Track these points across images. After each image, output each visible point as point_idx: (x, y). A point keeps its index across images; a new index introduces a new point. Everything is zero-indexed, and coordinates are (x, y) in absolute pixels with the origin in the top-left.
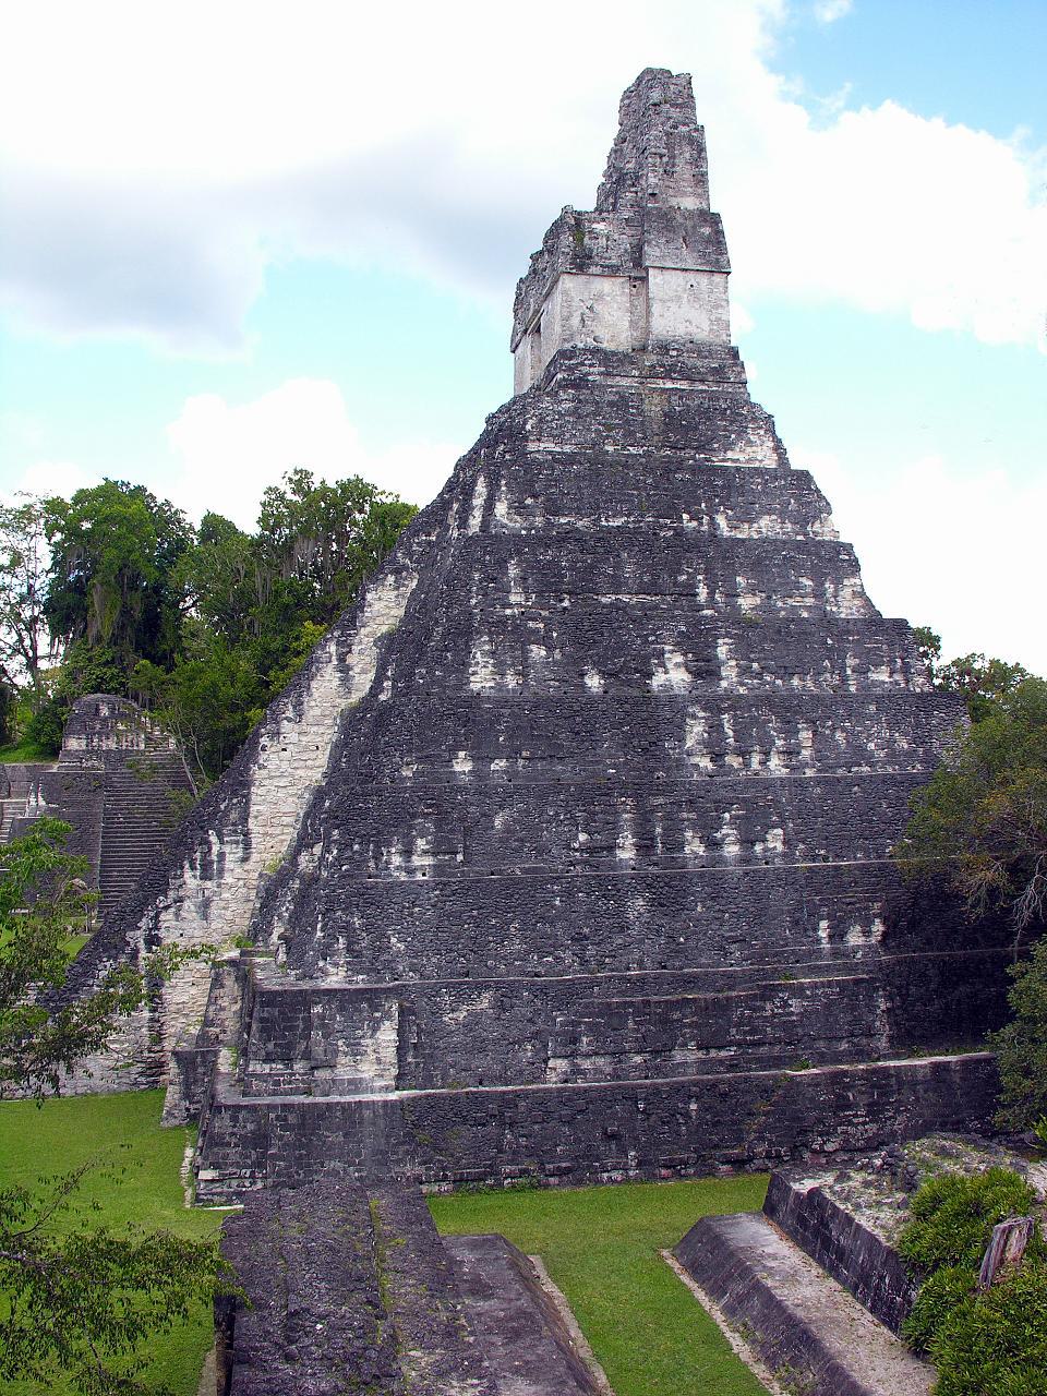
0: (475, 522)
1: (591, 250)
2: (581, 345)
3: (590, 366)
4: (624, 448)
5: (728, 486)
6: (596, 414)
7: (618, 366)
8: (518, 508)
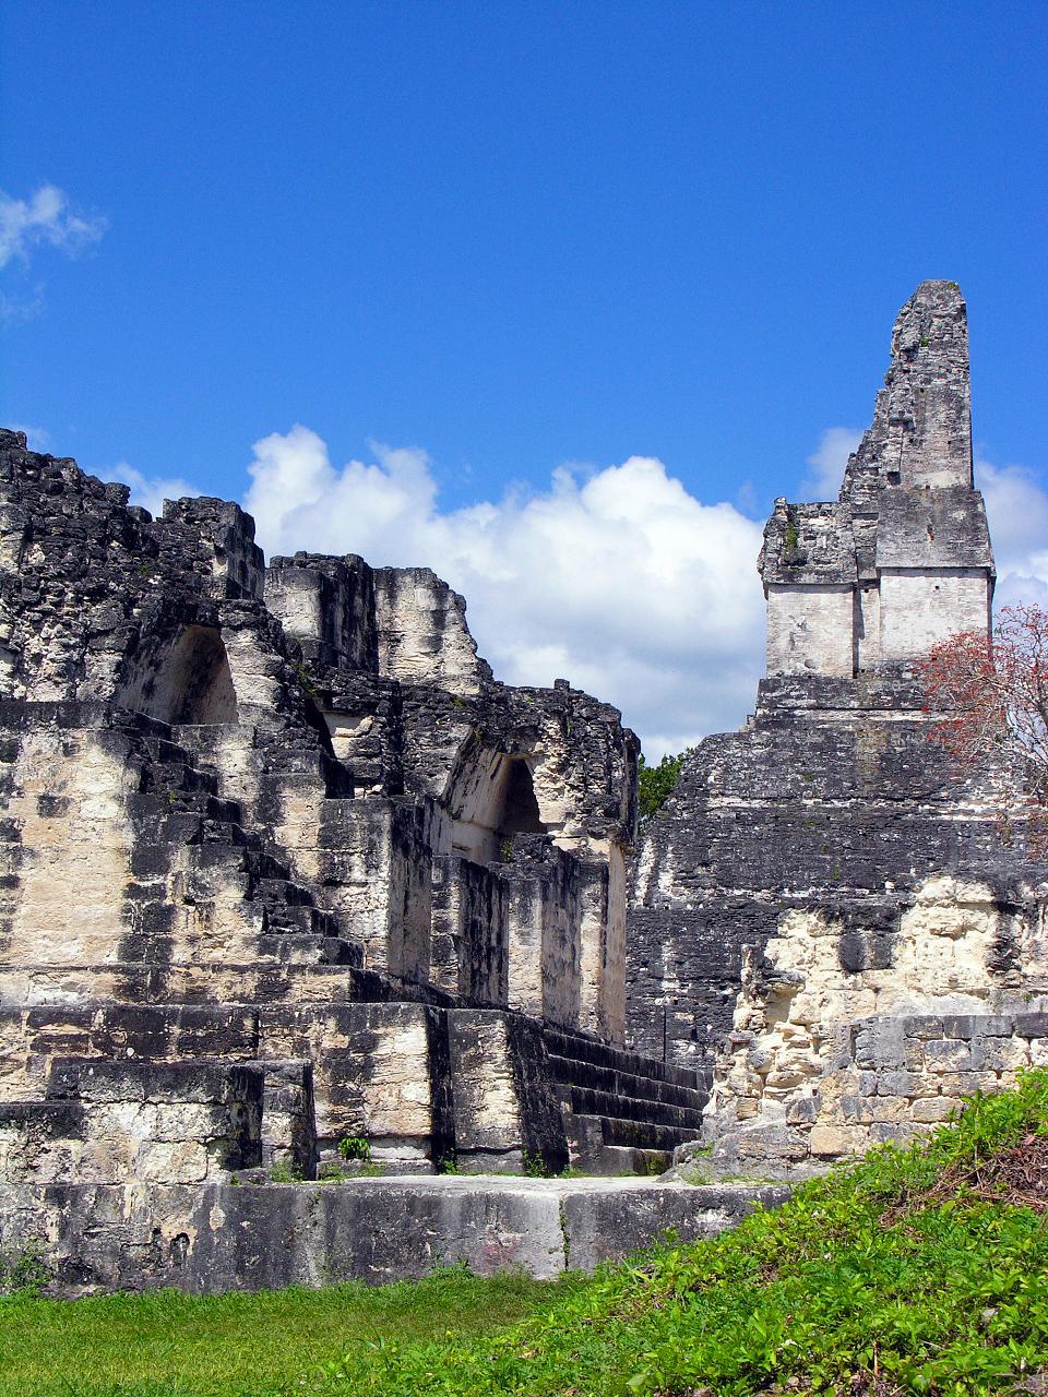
1: (805, 554)
2: (788, 673)
3: (798, 698)
4: (826, 800)
6: (793, 760)
7: (833, 696)
8: (686, 878)
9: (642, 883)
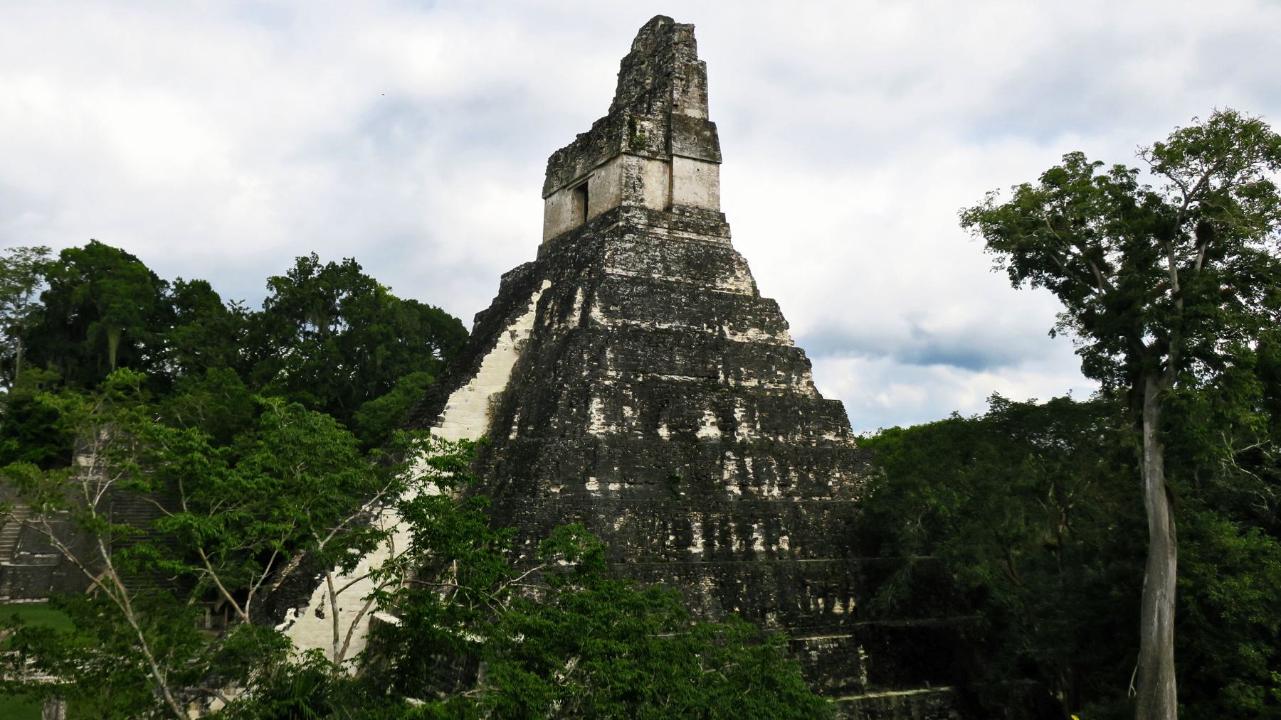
0: (575, 319)
5: (730, 306)
8: (605, 311)
9: (577, 314)
